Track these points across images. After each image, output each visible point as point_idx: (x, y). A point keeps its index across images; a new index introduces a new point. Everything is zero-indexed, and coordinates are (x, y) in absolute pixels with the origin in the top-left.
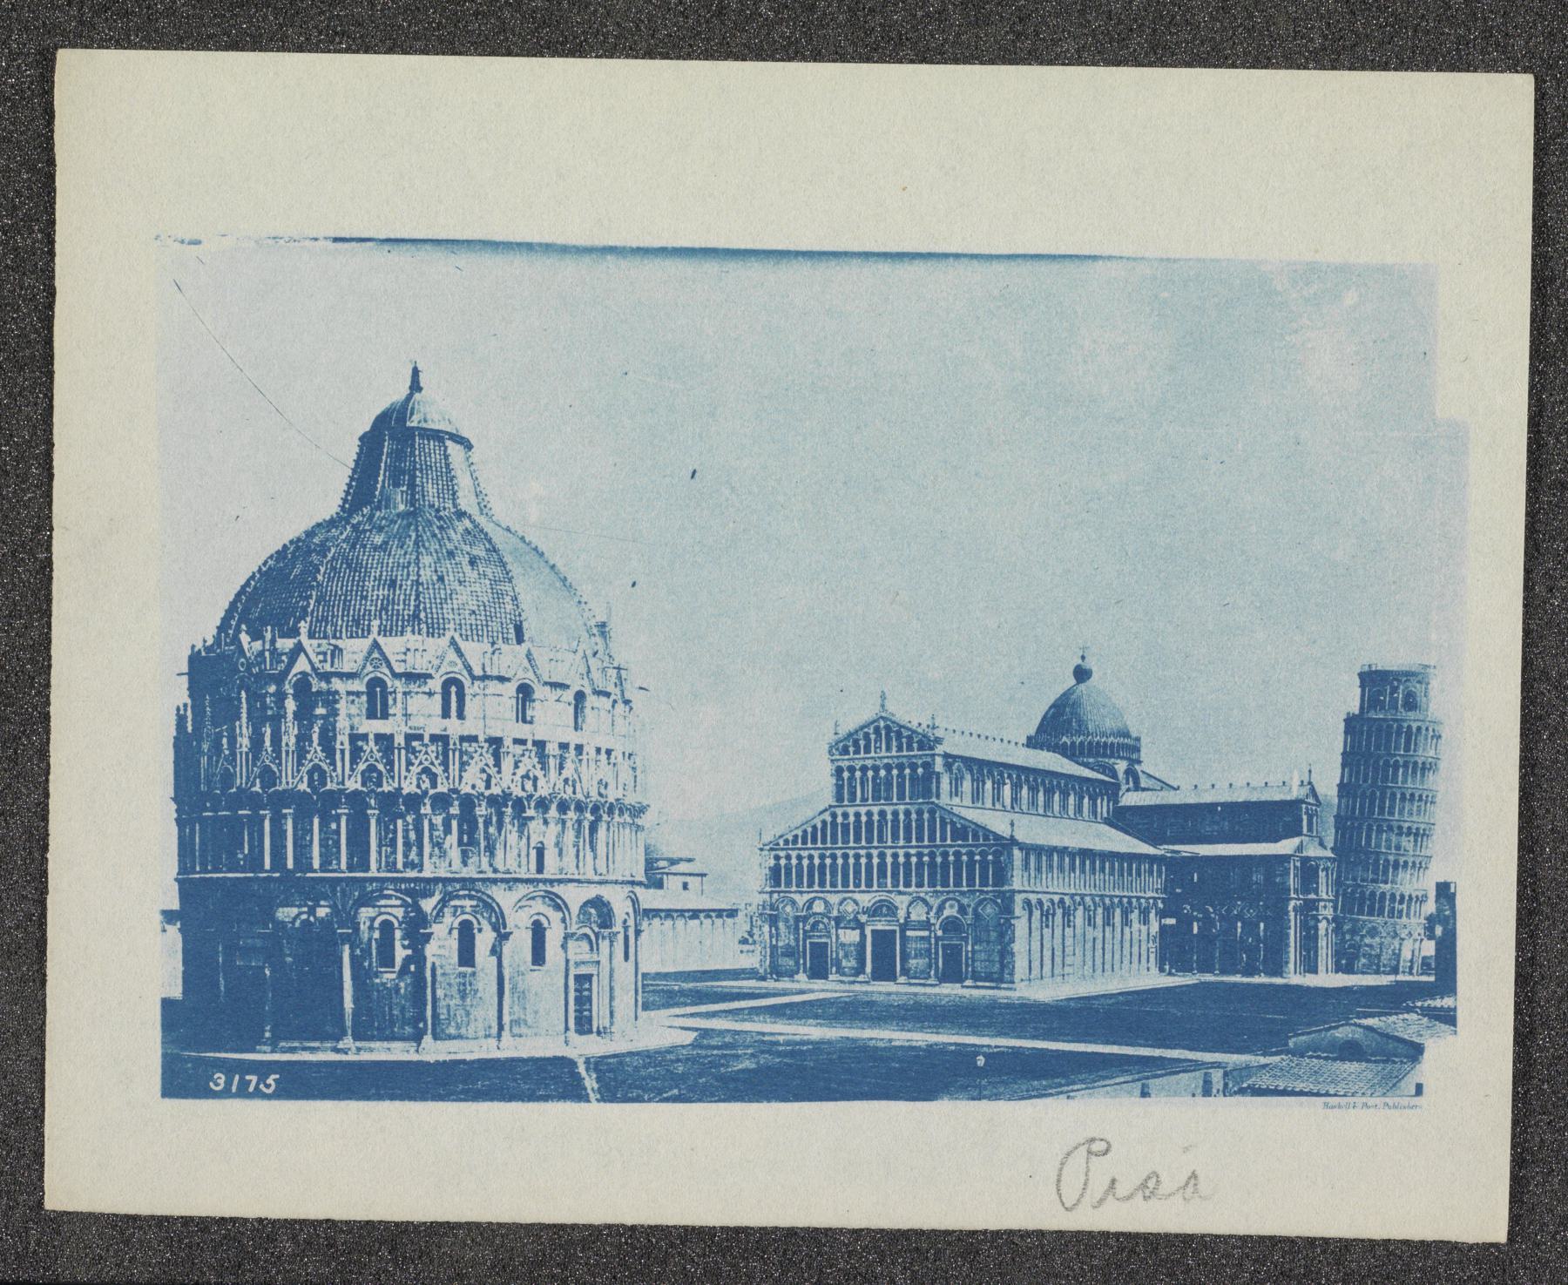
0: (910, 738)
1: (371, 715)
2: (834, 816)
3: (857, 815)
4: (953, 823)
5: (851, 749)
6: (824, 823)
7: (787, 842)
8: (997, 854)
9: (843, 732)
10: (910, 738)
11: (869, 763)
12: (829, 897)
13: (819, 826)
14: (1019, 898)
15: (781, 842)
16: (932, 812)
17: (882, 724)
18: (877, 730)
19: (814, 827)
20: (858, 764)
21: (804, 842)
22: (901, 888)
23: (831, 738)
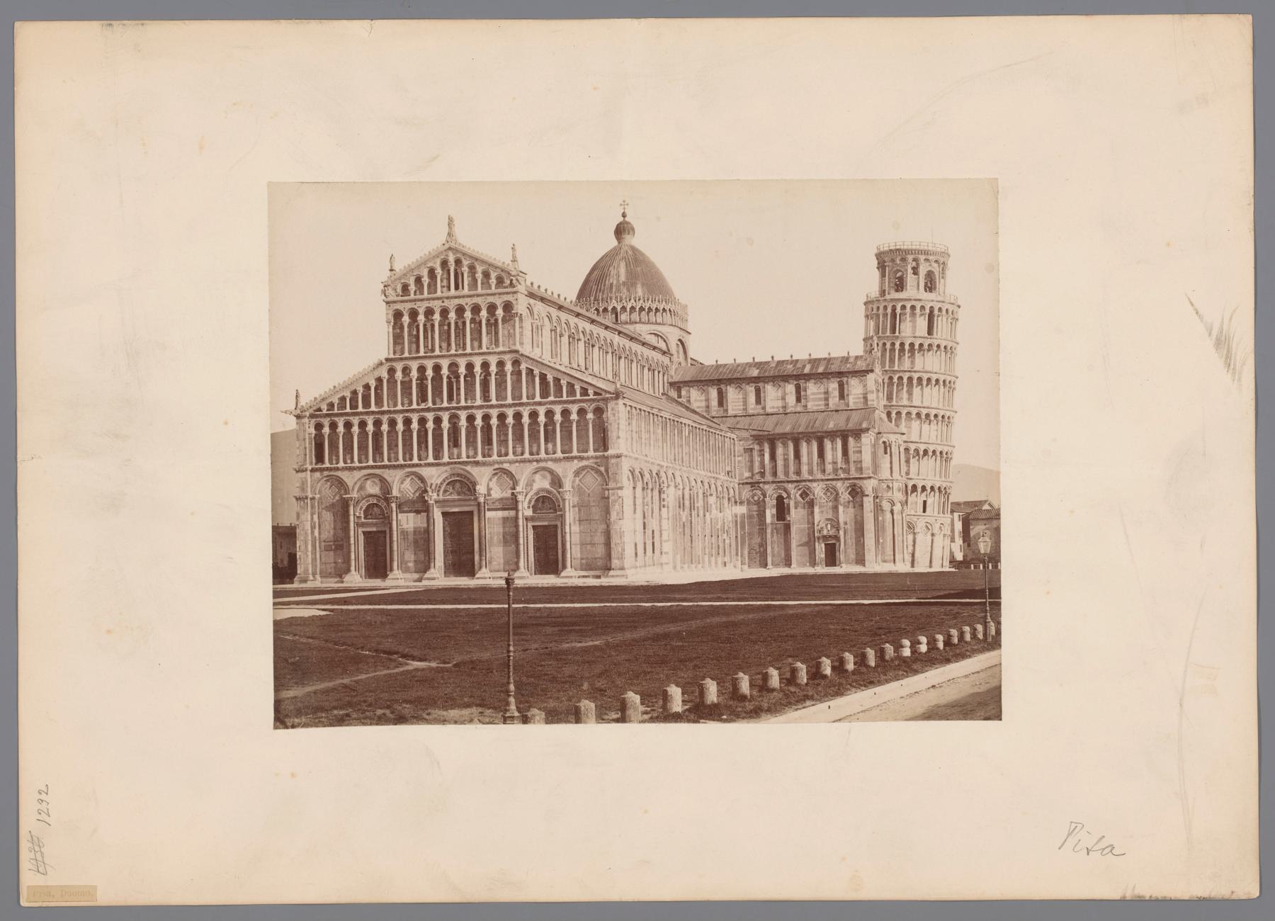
0: (486, 275)
2: (392, 371)
3: (422, 369)
4: (543, 377)
5: (412, 288)
6: (379, 380)
7: (331, 405)
8: (599, 411)
9: (399, 267)
10: (486, 275)
11: (437, 306)
12: (387, 474)
13: (373, 384)
14: (625, 465)
15: (324, 407)
16: (516, 363)
17: (451, 259)
18: (444, 264)
19: (367, 387)
21: (354, 406)
22: (480, 458)
23: (385, 275)
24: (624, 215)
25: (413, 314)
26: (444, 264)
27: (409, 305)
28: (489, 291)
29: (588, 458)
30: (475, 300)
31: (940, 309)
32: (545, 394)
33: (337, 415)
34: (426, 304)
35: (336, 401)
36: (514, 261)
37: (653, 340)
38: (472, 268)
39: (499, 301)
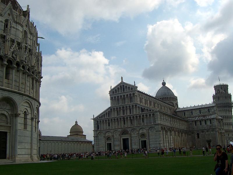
2: (111, 109)
7: (100, 118)
15: (98, 118)
16: (136, 106)
18: (121, 86)
20: (116, 96)
24: (164, 81)
25: (115, 97)
28: (130, 91)
29: (152, 125)
30: (127, 93)
31: (228, 96)
32: (142, 112)
33: (101, 119)
34: (117, 95)
35: (101, 116)
36: (135, 84)
37: (170, 104)
38: (126, 87)
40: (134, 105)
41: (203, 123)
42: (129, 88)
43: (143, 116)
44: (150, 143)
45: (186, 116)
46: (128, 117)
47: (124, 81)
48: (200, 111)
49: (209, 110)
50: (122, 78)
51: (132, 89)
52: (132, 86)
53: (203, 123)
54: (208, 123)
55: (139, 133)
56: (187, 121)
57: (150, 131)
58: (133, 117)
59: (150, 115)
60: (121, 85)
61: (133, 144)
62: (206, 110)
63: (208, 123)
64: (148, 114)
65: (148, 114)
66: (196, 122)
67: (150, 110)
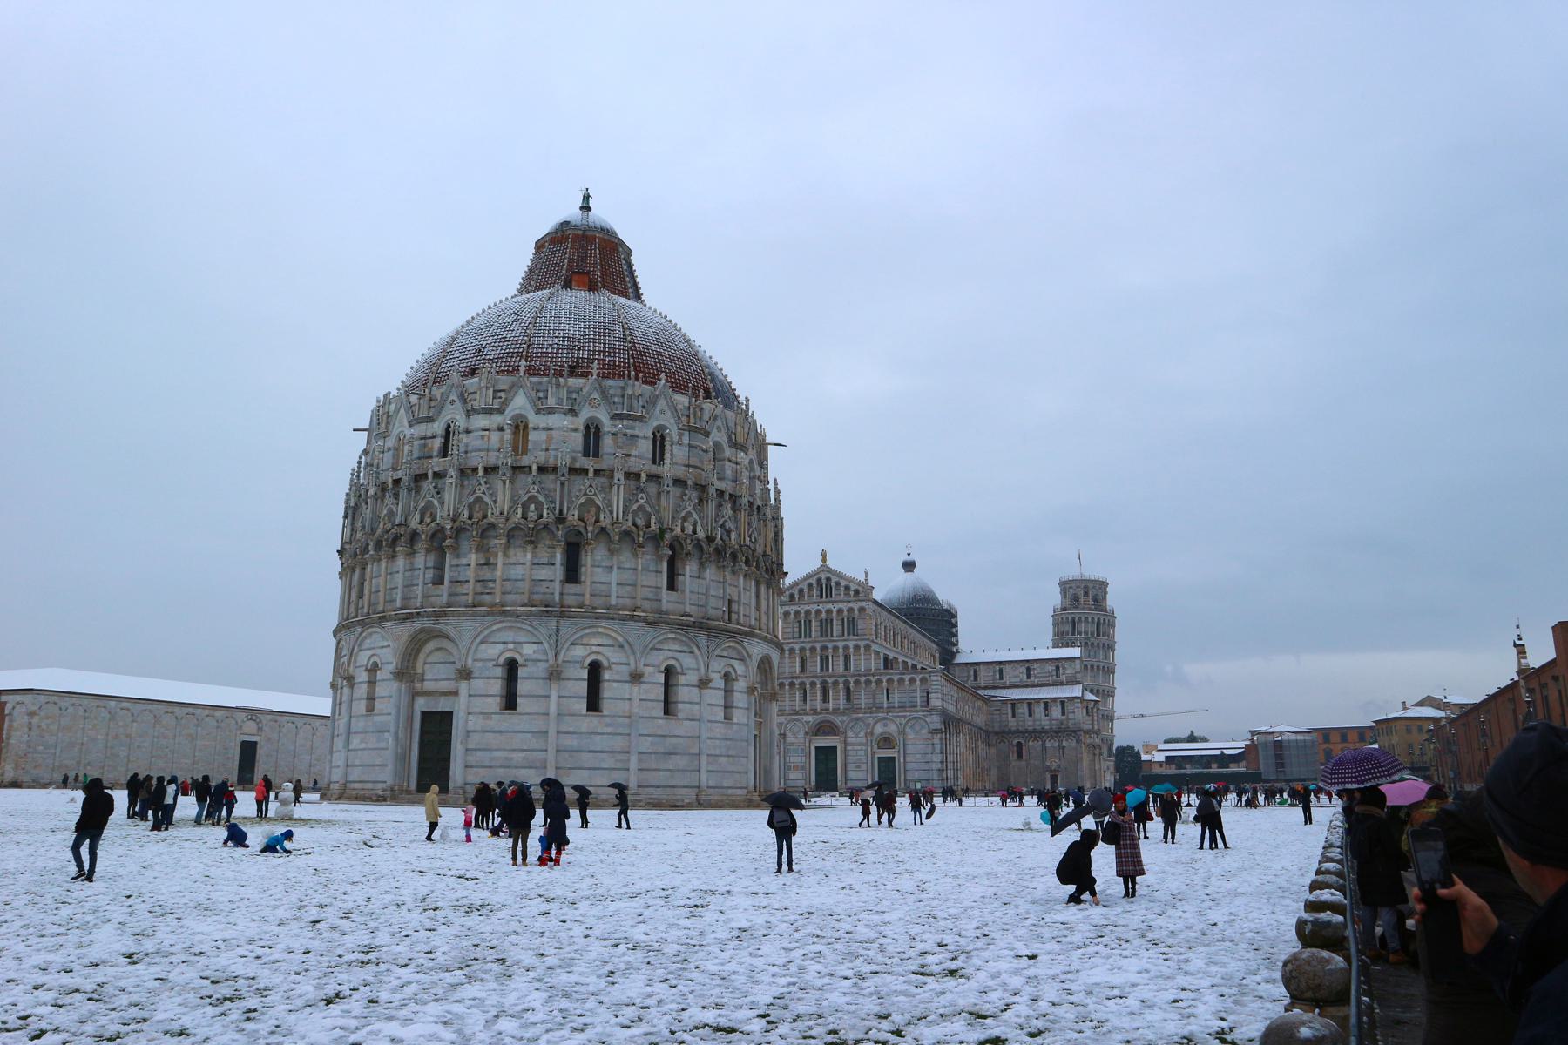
1: (586, 454)
18: (819, 580)
26: (819, 580)
27: (795, 608)
30: (841, 605)
32: (886, 667)
38: (838, 584)
39: (856, 606)
40: (862, 644)
41: (1039, 710)
42: (847, 588)
43: (890, 681)
44: (909, 766)
45: (982, 682)
46: (841, 680)
47: (831, 563)
48: (1028, 669)
49: (1058, 668)
50: (824, 555)
51: (857, 592)
52: (859, 583)
53: (1039, 710)
54: (1056, 712)
55: (872, 734)
56: (986, 700)
57: (908, 730)
58: (857, 682)
59: (912, 681)
60: (823, 576)
61: (850, 766)
62: (1050, 668)
63: (1056, 712)
64: (907, 678)
65: (907, 678)
66: (1014, 704)
67: (914, 667)
